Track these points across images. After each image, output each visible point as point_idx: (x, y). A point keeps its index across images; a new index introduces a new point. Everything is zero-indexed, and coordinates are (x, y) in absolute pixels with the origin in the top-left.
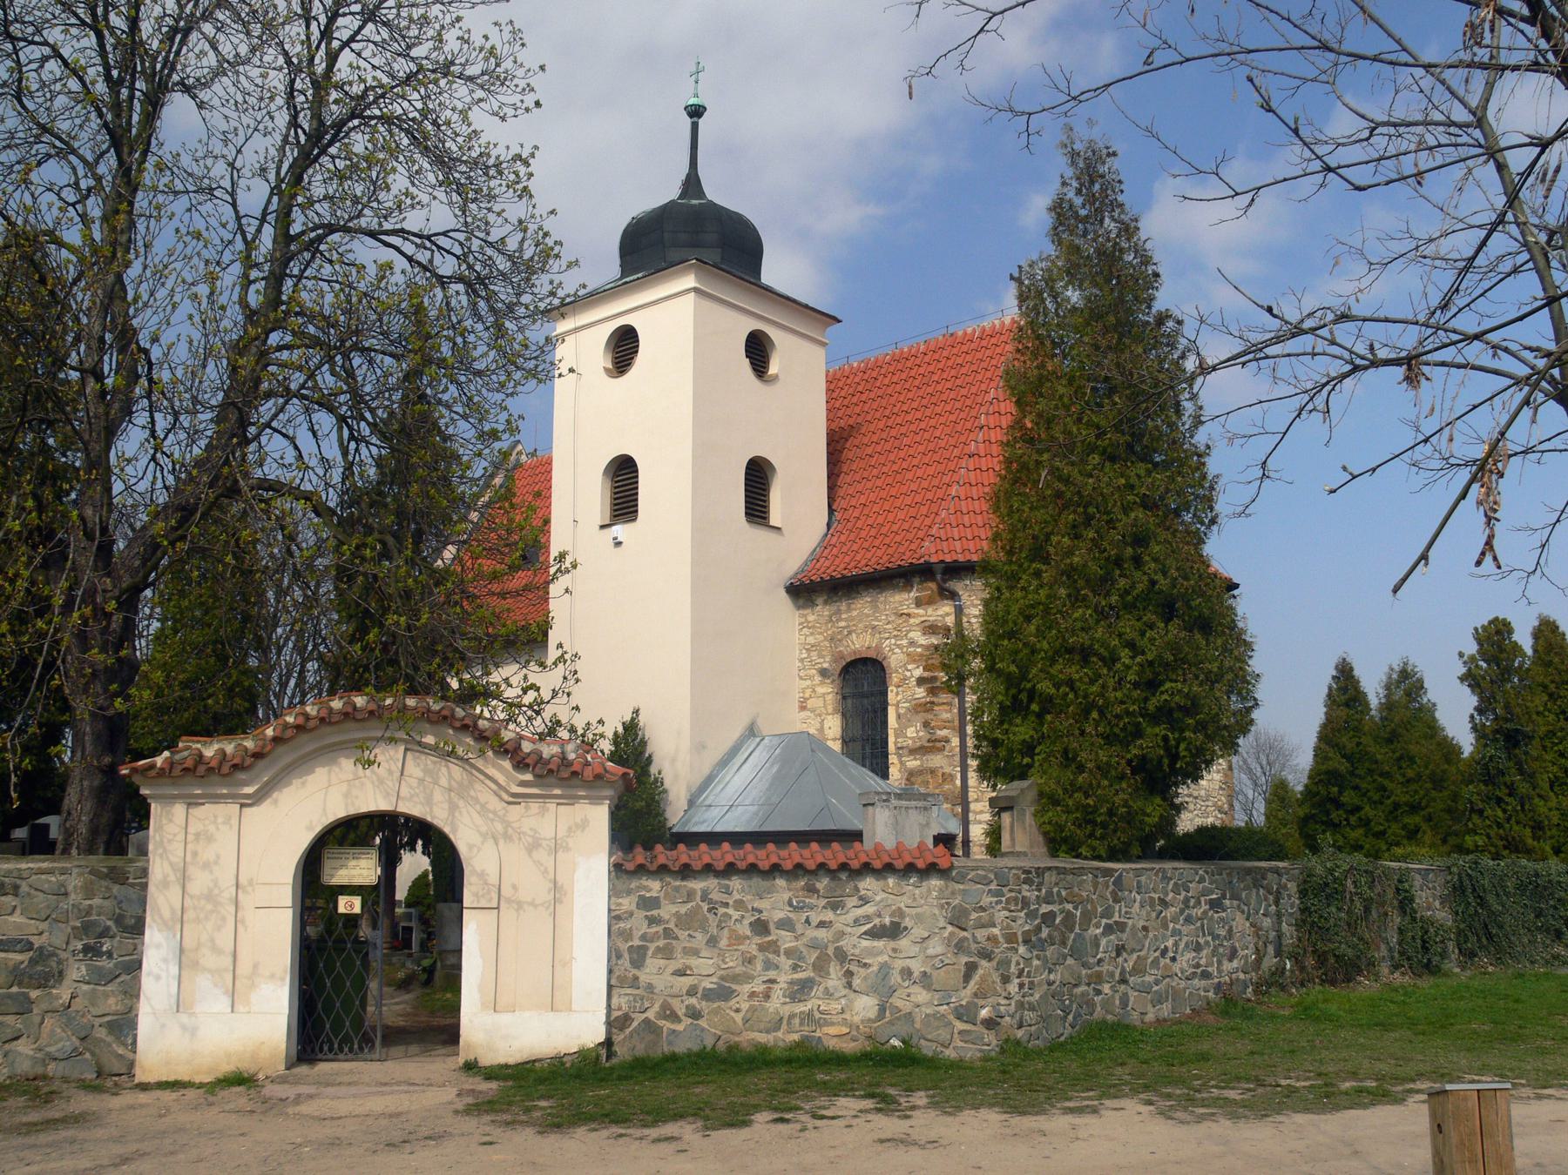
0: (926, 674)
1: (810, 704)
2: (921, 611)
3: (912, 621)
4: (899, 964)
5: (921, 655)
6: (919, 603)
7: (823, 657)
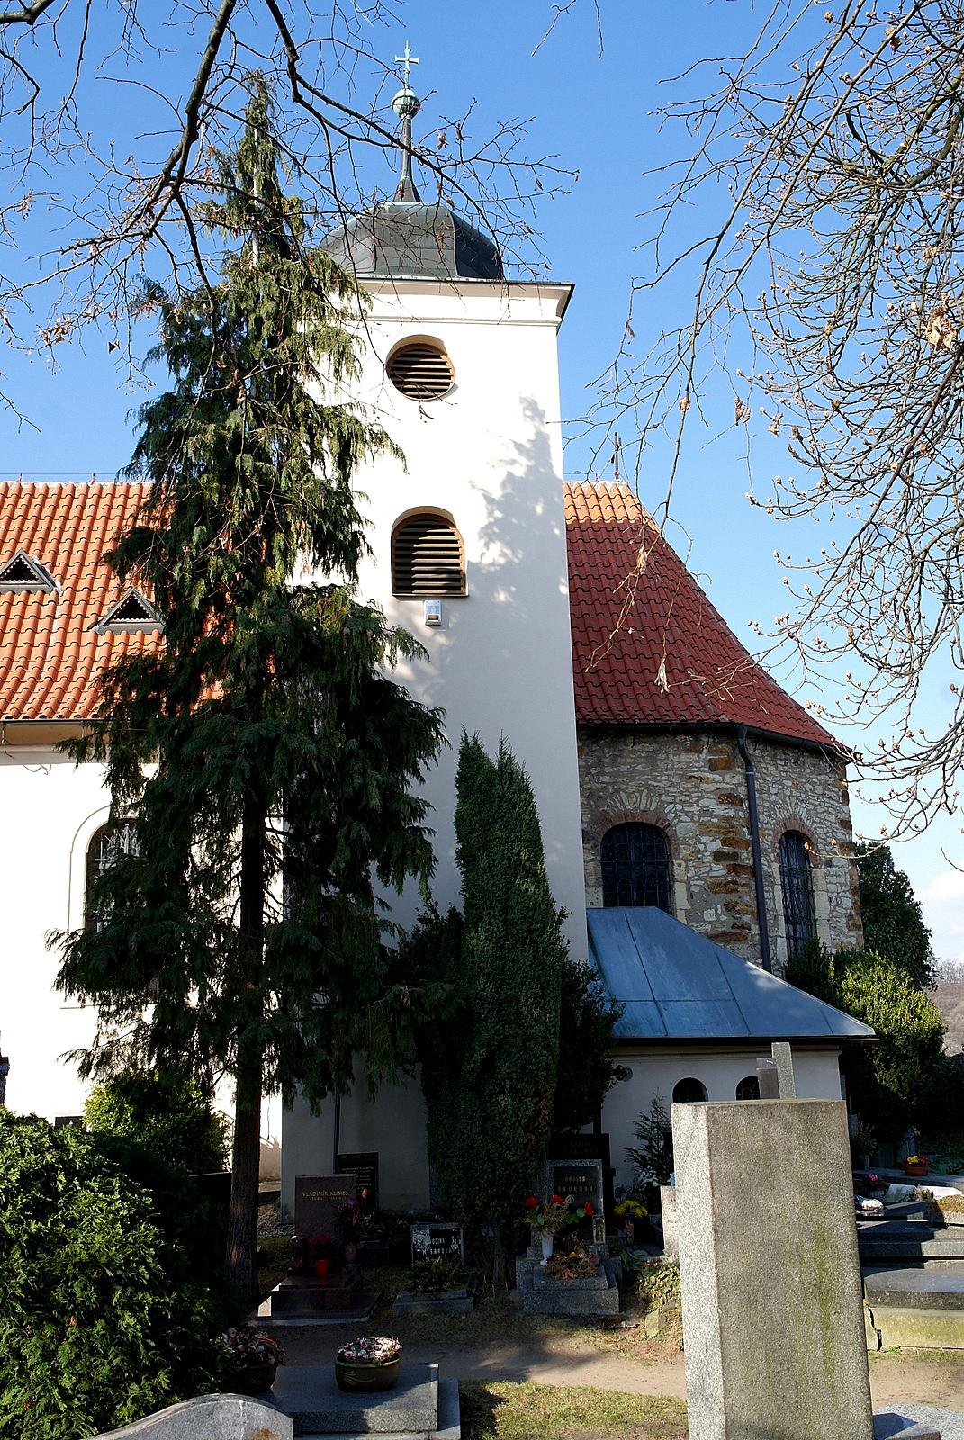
0: (726, 849)
2: (717, 777)
3: (704, 786)
6: (713, 767)
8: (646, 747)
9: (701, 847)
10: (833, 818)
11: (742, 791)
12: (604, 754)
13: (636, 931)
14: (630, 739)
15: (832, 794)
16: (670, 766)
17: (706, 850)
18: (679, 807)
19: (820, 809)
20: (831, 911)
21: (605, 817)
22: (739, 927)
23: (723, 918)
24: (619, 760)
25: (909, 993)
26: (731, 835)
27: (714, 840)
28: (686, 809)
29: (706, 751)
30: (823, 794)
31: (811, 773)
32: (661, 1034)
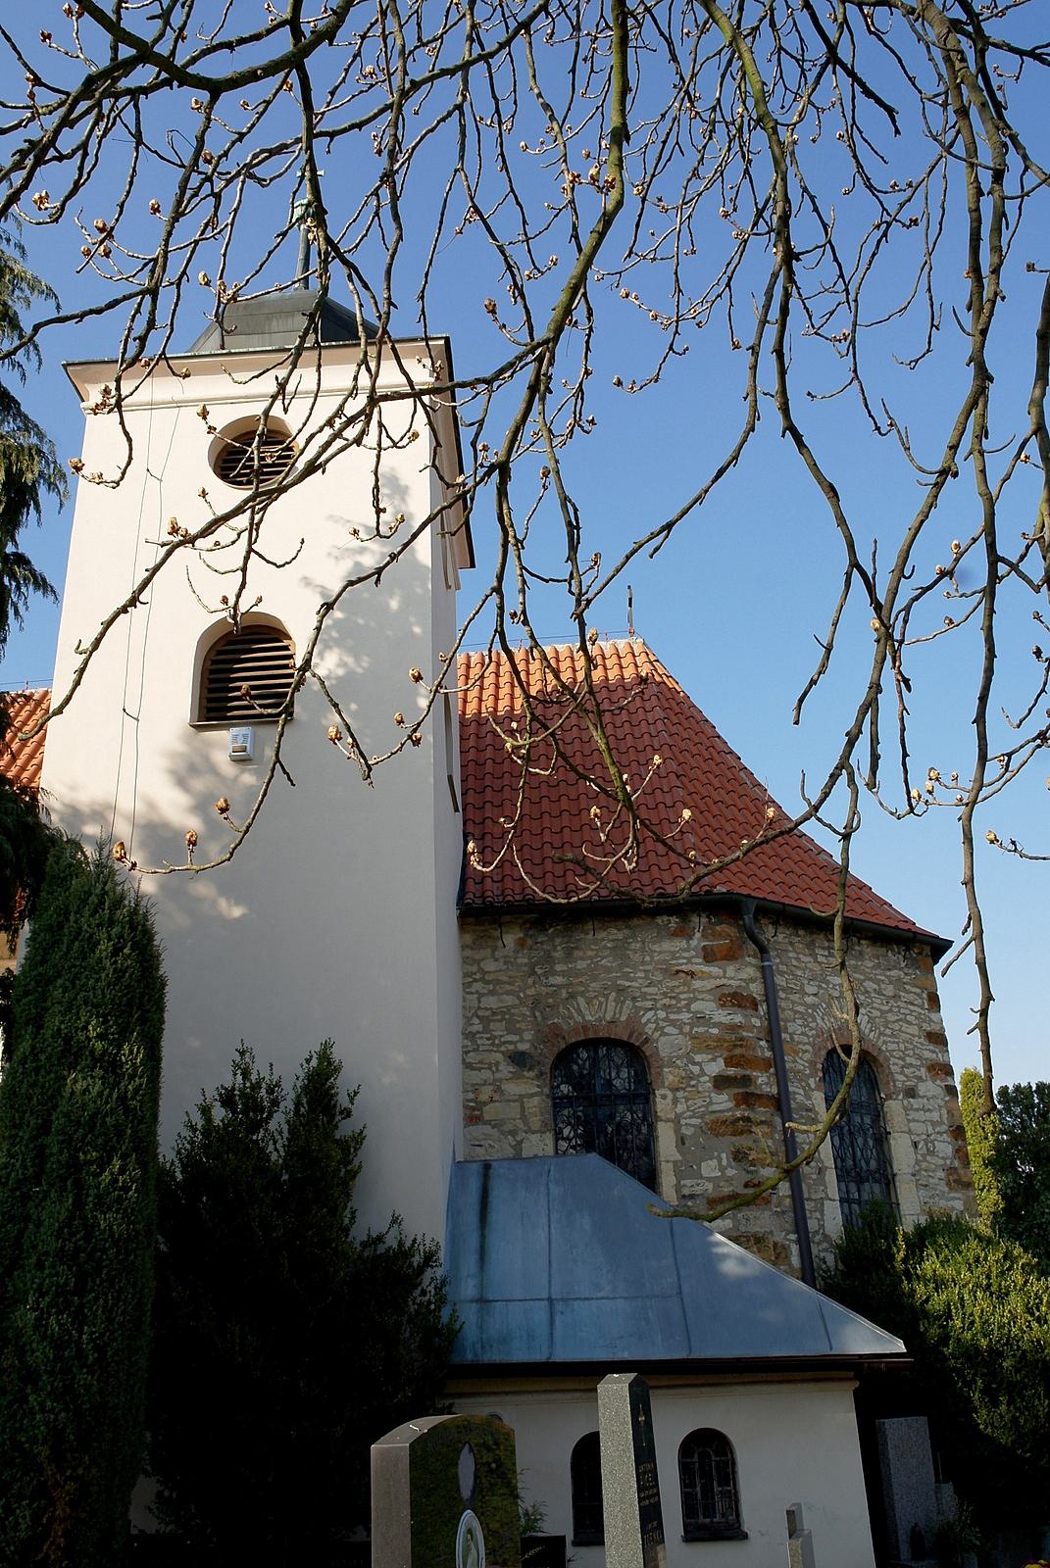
0: (731, 1071)
1: (489, 1112)
2: (714, 970)
3: (697, 984)
5: (719, 1040)
6: (709, 956)
7: (519, 1032)
8: (614, 934)
9: (696, 1069)
10: (914, 1030)
11: (756, 989)
12: (555, 947)
13: (555, 1190)
14: (590, 926)
15: (911, 997)
16: (647, 958)
17: (703, 1073)
18: (662, 1014)
19: (891, 1017)
20: (917, 1162)
21: (556, 1032)
22: (755, 1186)
23: (731, 1172)
24: (577, 953)
25: (1026, 1282)
26: (738, 1051)
27: (714, 1060)
28: (672, 1017)
29: (698, 935)
30: (896, 997)
31: (875, 967)
32: (539, 1356)
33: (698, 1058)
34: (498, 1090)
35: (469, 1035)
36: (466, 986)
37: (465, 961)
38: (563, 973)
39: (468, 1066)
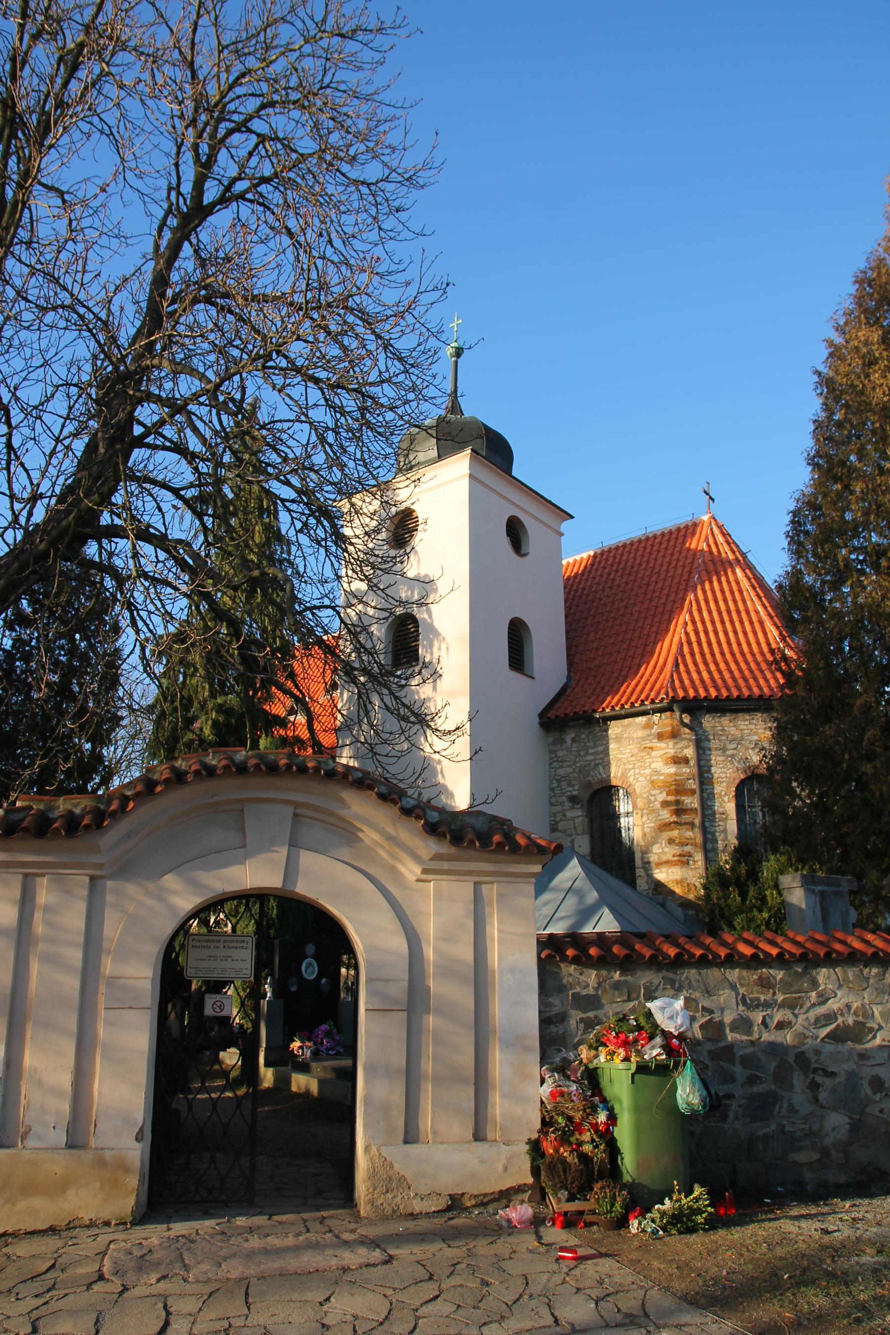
0: (670, 798)
1: (561, 825)
2: (662, 745)
3: (654, 753)
4: (867, 1073)
5: (664, 782)
7: (573, 786)
17: (656, 800)
18: (637, 771)
33: (654, 792)
34: (564, 815)
35: (552, 789)
36: (551, 764)
37: (551, 752)
38: (592, 754)
39: (552, 804)
